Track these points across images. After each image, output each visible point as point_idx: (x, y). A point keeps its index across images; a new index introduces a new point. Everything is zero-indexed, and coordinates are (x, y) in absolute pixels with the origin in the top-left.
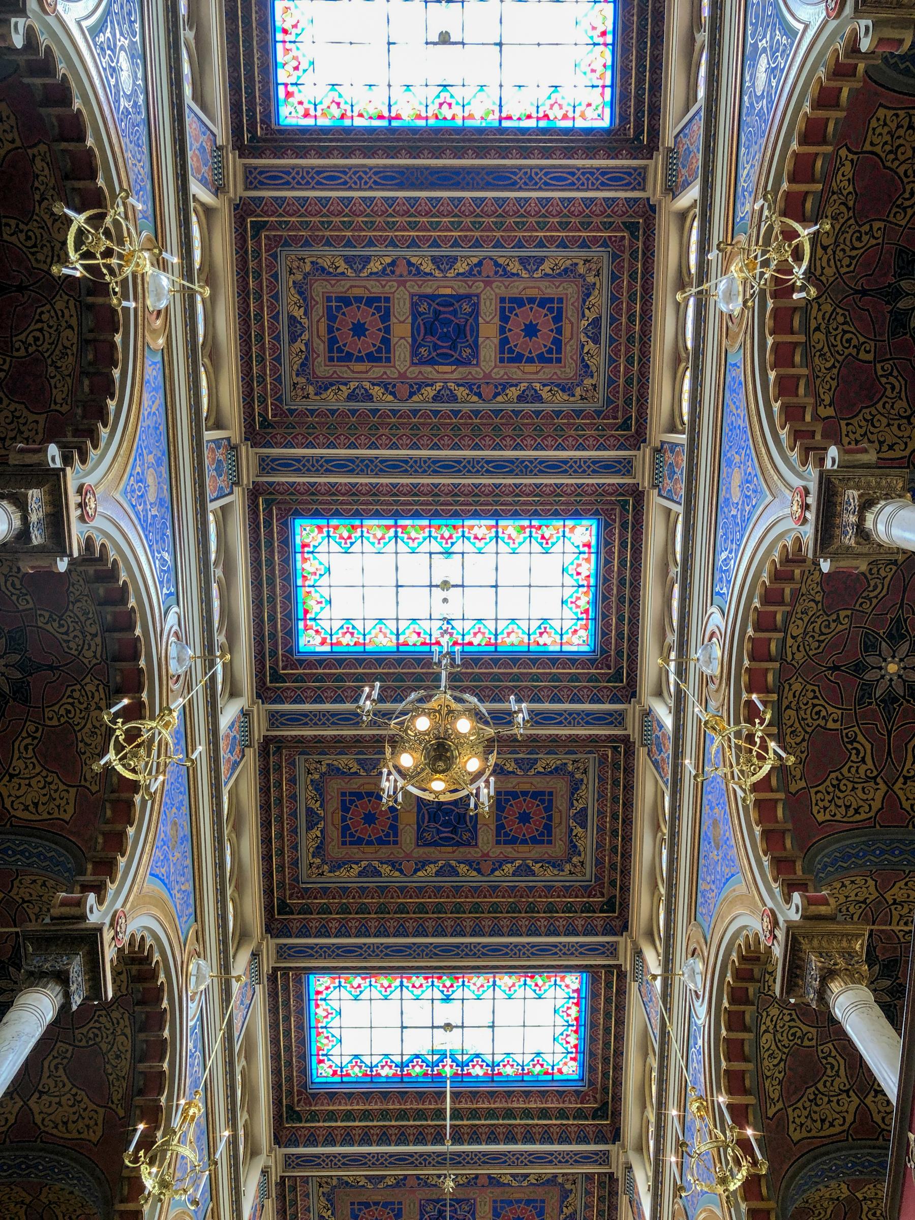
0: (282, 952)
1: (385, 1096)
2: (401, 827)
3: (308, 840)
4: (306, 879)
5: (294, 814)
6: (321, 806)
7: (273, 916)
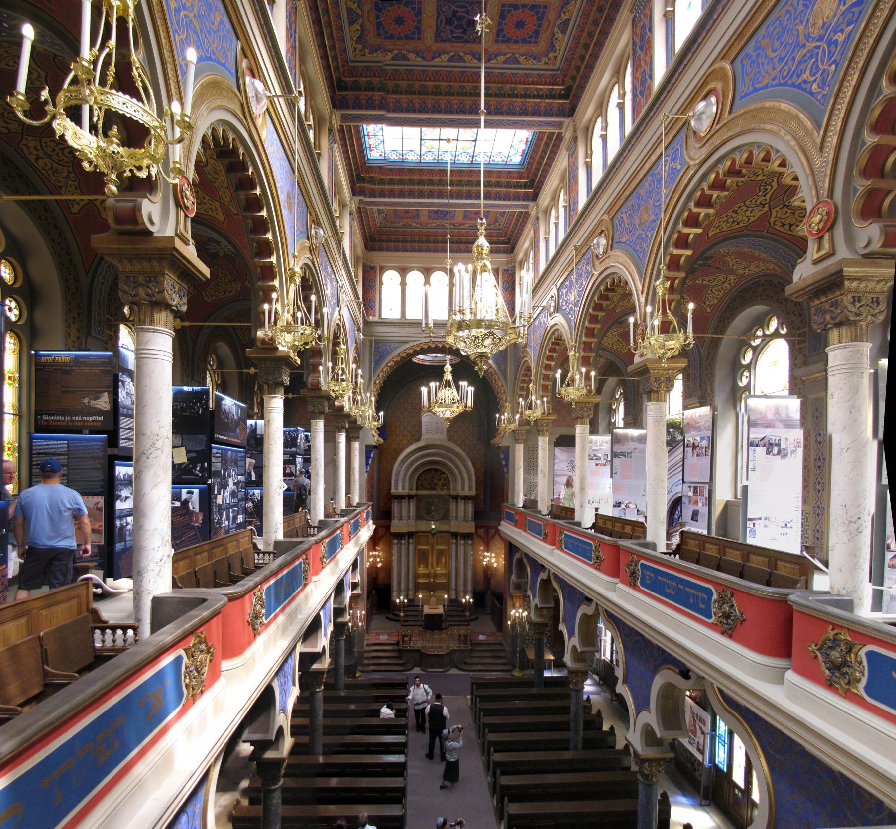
0: (344, 118)
1: (411, 171)
2: (423, 28)
3: (350, 33)
4: (353, 59)
5: (338, 17)
6: (358, 7)
7: (334, 91)
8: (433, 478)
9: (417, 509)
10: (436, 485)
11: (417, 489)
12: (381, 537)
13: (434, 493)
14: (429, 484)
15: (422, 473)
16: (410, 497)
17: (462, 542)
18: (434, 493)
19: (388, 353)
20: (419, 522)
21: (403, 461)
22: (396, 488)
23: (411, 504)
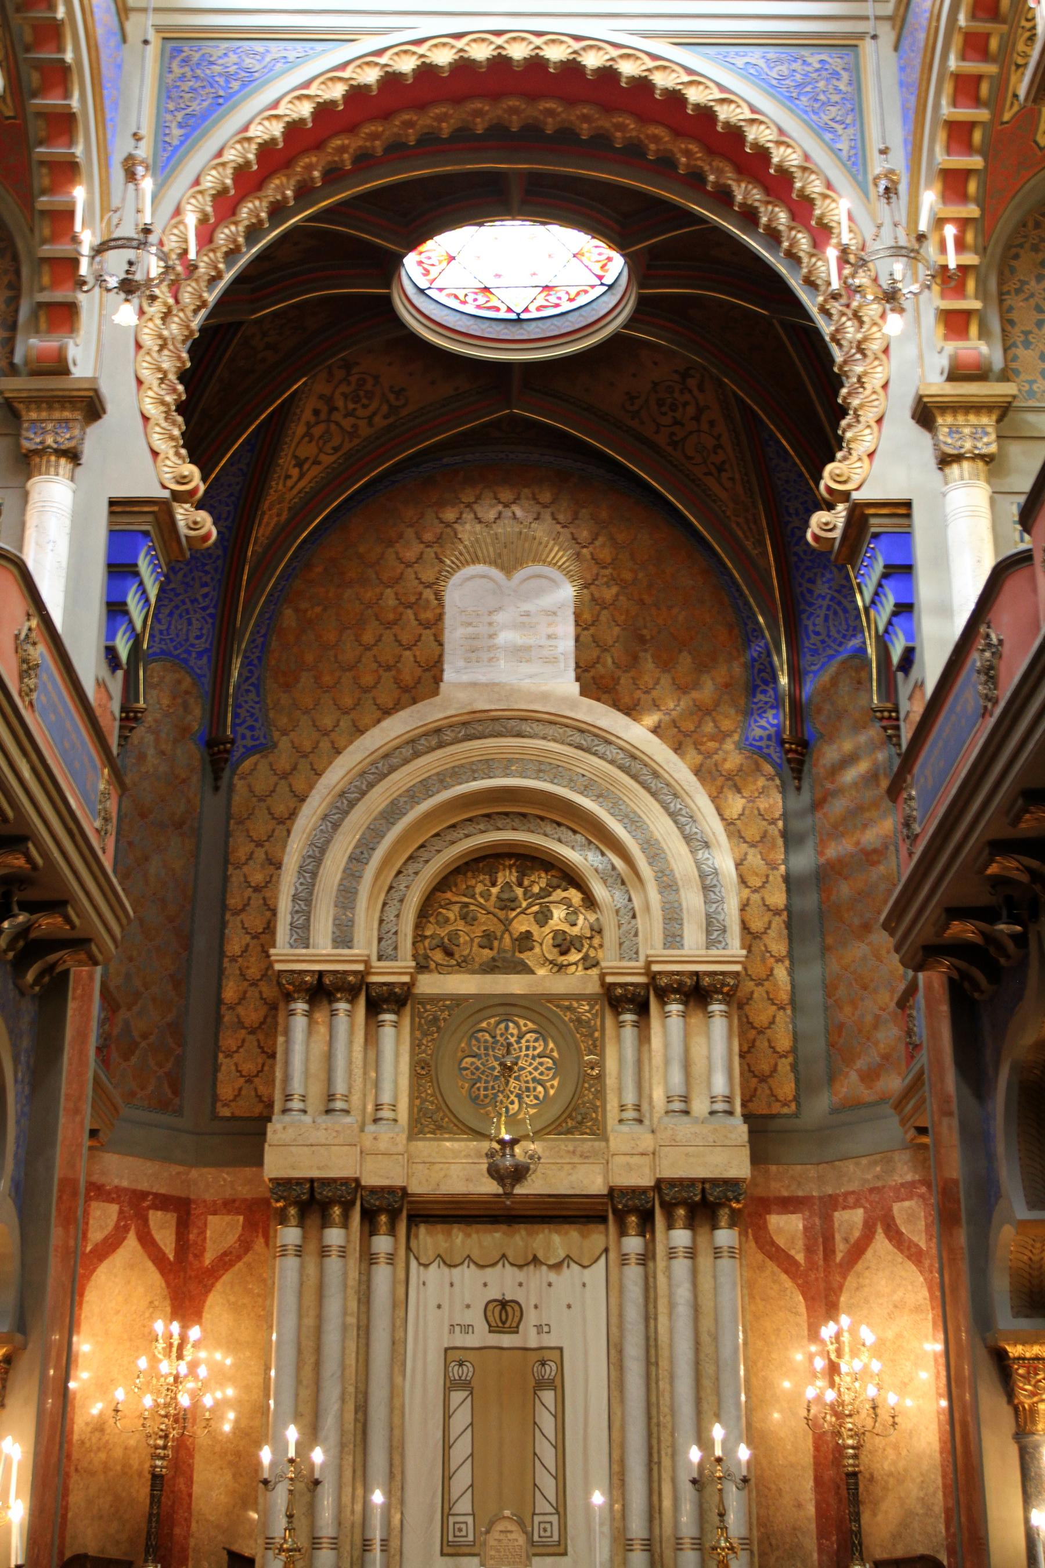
8: (508, 903)
9: (423, 1070)
10: (525, 941)
11: (422, 967)
12: (226, 1261)
13: (514, 984)
14: (488, 939)
15: (444, 883)
16: (383, 1001)
17: (681, 1237)
18: (514, 984)
19: (250, 81)
20: (424, 1147)
21: (346, 800)
22: (302, 934)
23: (388, 1033)
